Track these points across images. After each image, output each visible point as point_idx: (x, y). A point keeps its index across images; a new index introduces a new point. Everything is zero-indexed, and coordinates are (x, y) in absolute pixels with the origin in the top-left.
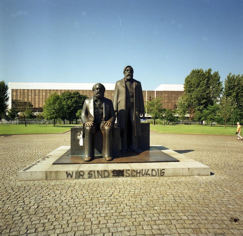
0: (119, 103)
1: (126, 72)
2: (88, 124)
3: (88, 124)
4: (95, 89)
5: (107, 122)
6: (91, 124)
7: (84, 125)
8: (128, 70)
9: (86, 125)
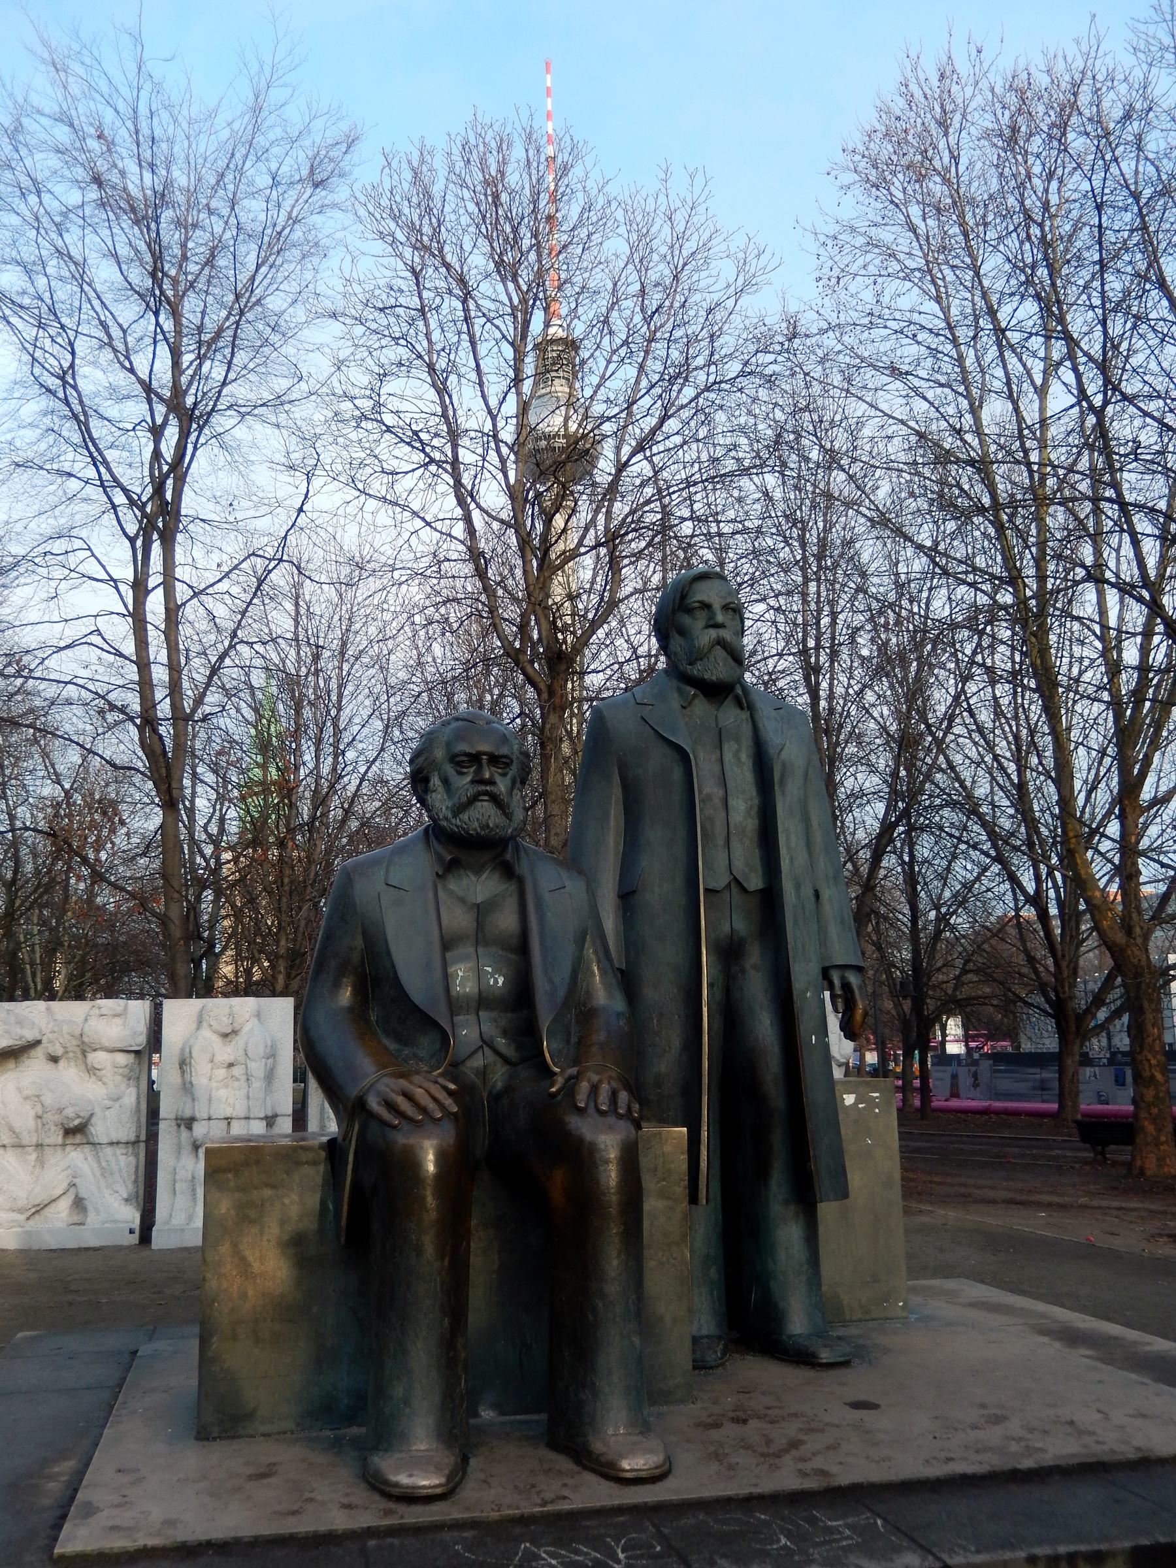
2: (407, 1096)
3: (407, 1096)
6: (435, 1099)
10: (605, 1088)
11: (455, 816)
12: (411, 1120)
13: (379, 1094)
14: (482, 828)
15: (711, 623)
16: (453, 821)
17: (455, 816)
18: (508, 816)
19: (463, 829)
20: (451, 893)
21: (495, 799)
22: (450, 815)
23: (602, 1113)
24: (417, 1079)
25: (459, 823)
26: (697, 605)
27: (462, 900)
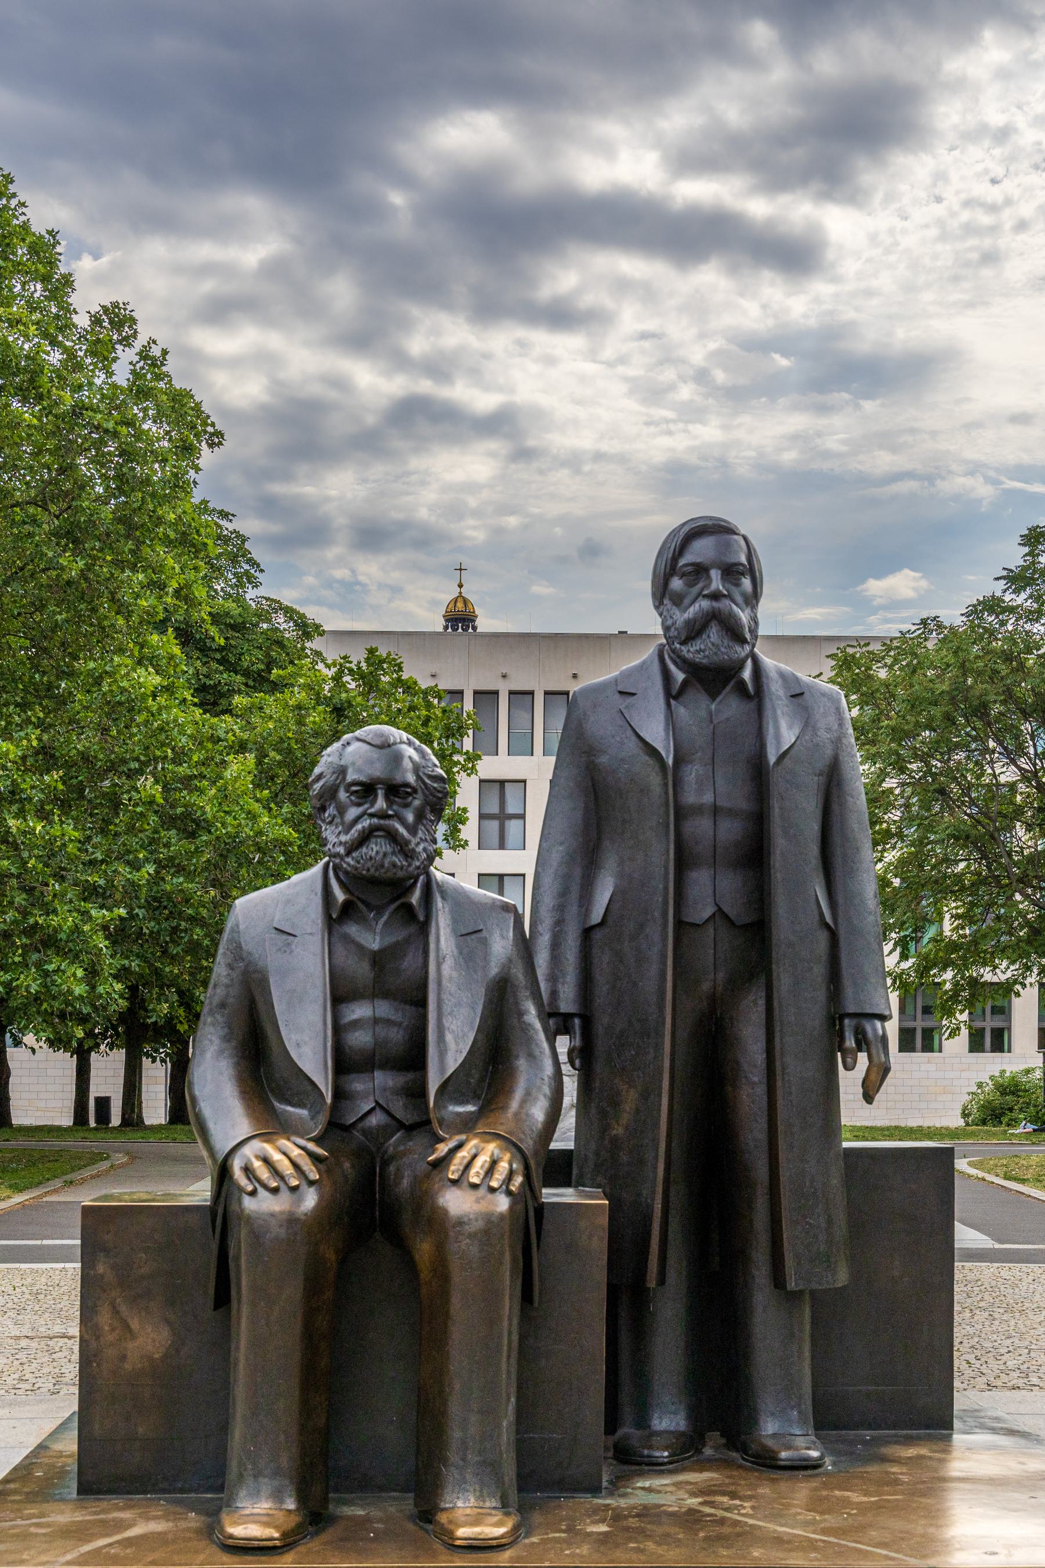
0: (602, 923)
1: (676, 584)
2: (266, 1161)
3: (266, 1161)
4: (342, 795)
5: (459, 1146)
7: (223, 1173)
8: (700, 571)
9: (248, 1170)
10: (483, 1160)
11: (349, 853)
12: (265, 1187)
13: (245, 1156)
14: (377, 870)
15: (706, 592)
16: (349, 860)
17: (349, 853)
18: (409, 854)
19: (356, 869)
20: (347, 939)
21: (392, 836)
22: (341, 850)
23: (475, 1187)
24: (284, 1143)
25: (352, 863)
26: (690, 569)
27: (360, 947)
